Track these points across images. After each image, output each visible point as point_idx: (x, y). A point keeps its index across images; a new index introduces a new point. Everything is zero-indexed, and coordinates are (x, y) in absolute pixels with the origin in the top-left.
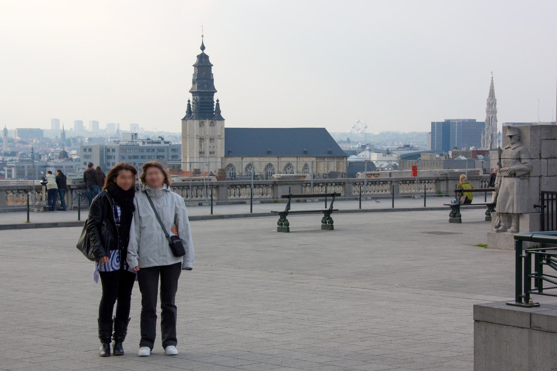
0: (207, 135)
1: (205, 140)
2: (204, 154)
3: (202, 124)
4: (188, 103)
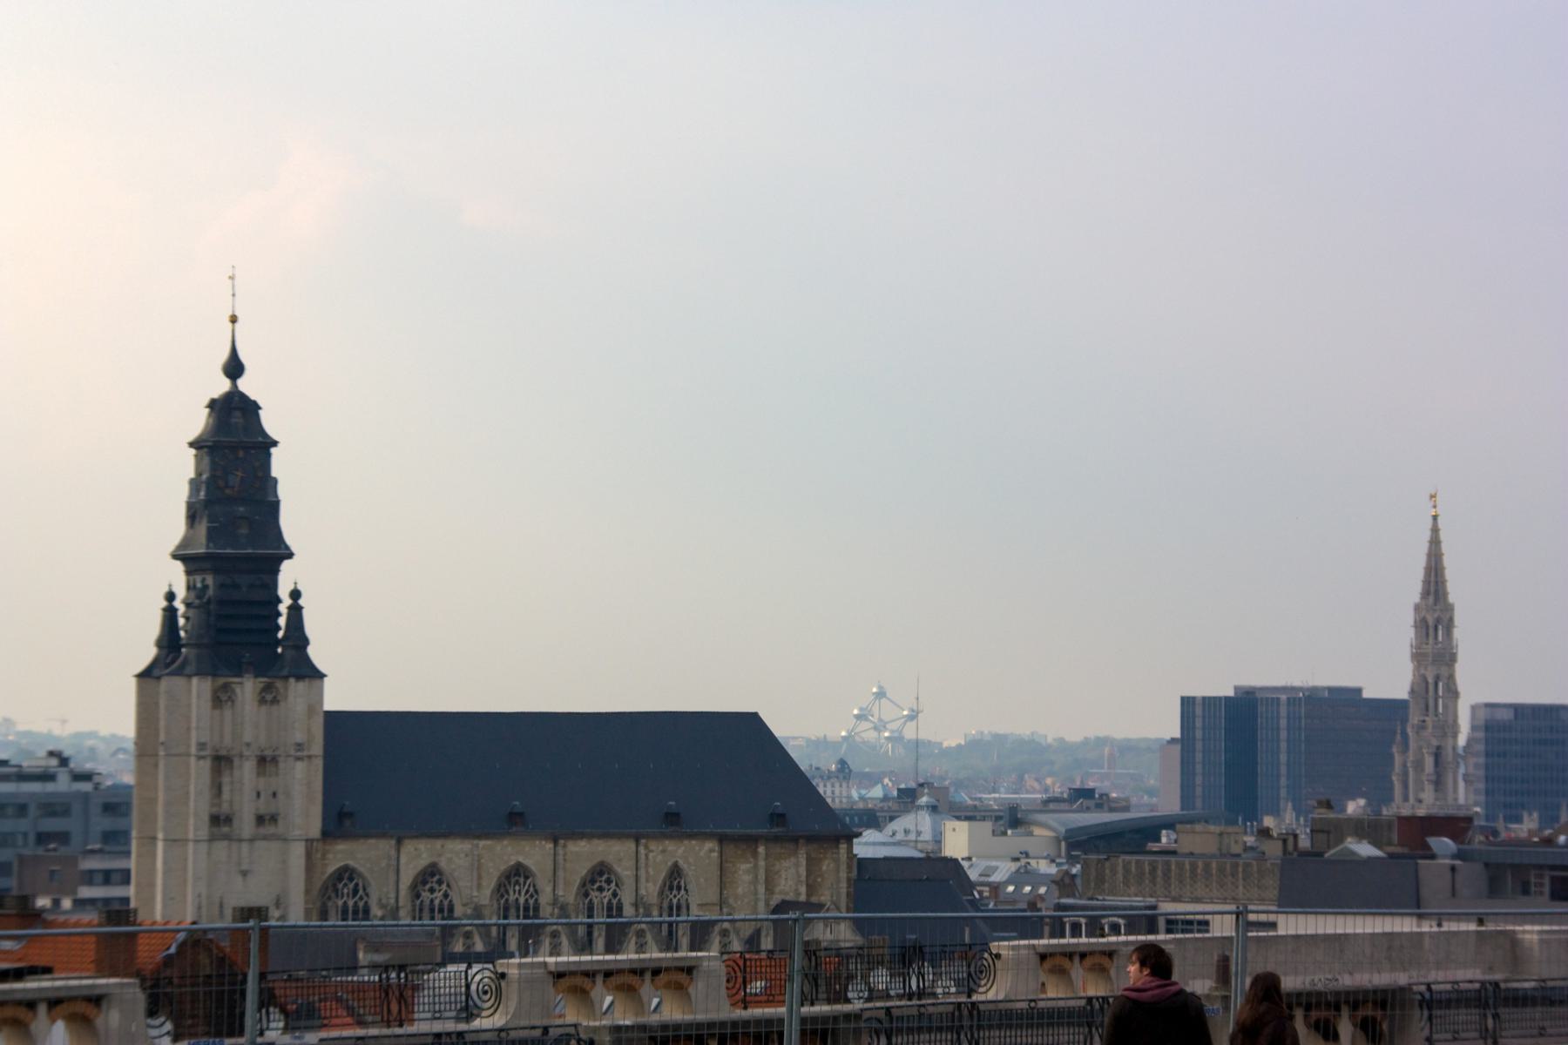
0: (248, 745)
3: (221, 698)
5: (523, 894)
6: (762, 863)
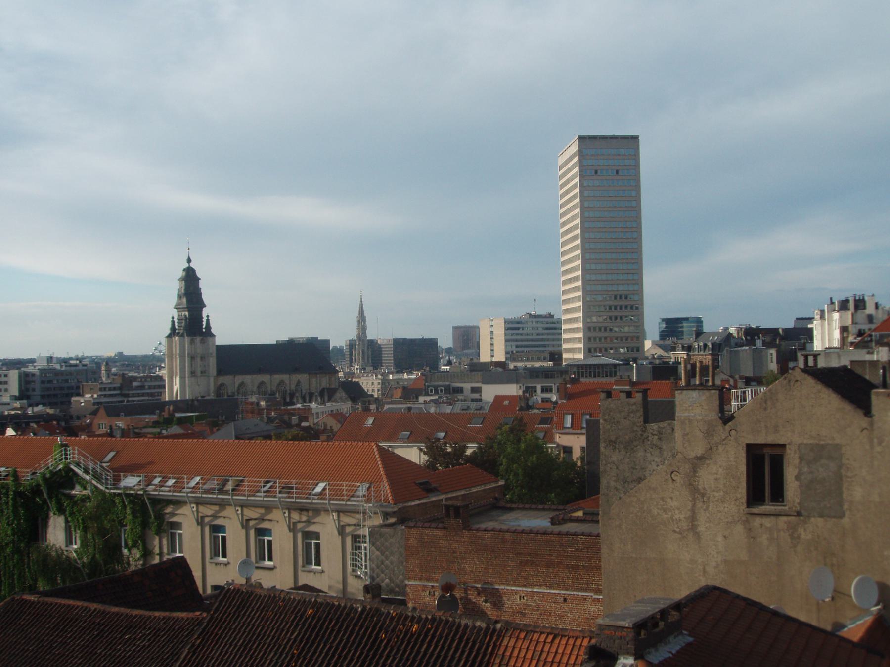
3: (192, 342)
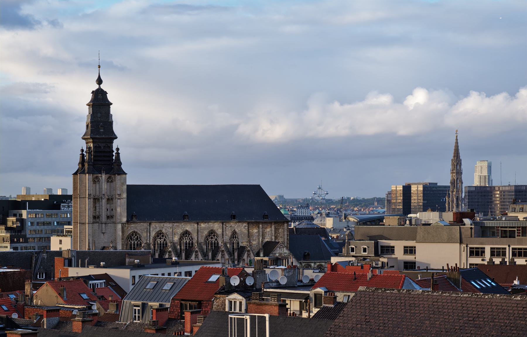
0: (104, 195)
1: (100, 200)
2: (99, 219)
3: (96, 181)
4: (81, 153)
5: (188, 239)
6: (261, 230)
